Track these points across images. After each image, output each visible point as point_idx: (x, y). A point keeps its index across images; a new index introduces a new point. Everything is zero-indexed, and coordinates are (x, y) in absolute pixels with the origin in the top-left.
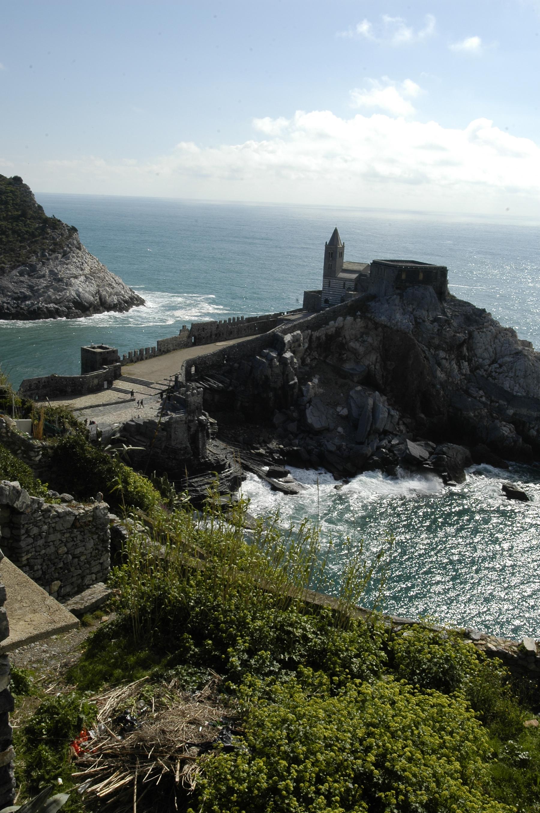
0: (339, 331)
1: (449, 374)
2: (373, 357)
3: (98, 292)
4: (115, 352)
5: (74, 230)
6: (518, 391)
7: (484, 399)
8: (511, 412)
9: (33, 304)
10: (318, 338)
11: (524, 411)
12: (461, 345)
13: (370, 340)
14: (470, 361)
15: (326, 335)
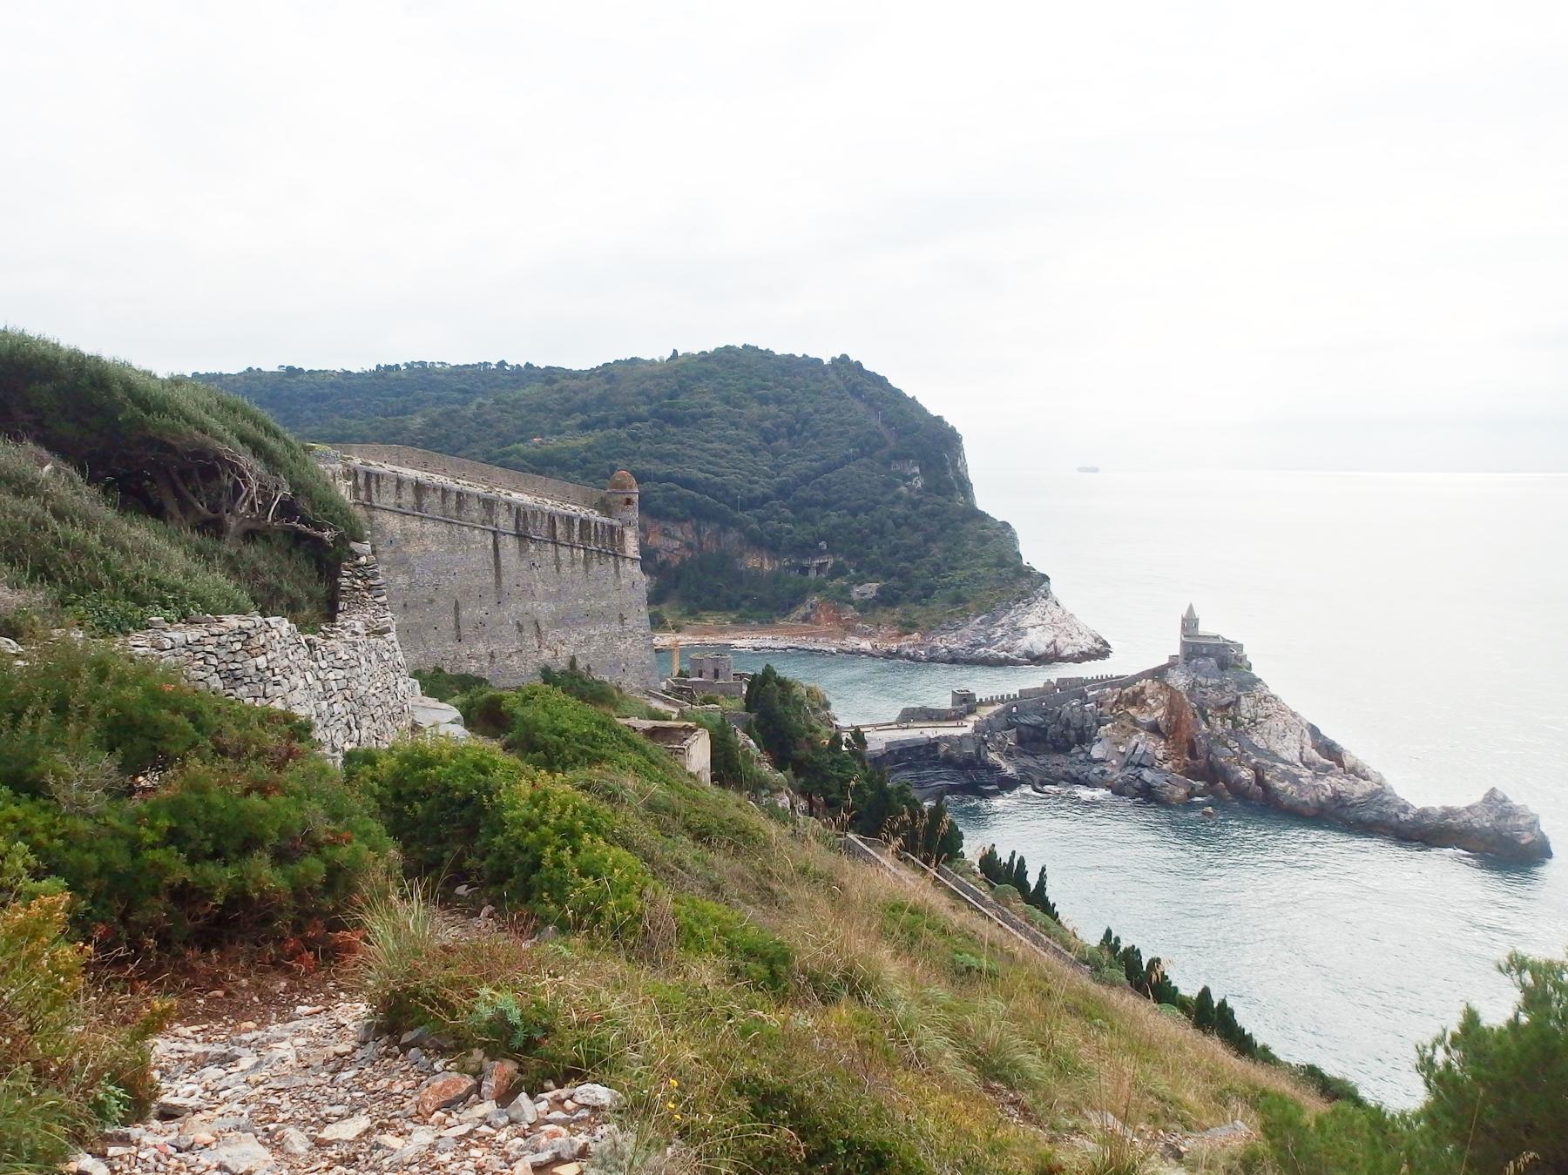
0: (1143, 689)
1: (1213, 729)
2: (1161, 712)
3: (1053, 642)
4: (973, 695)
5: (1045, 578)
6: (1262, 745)
7: (1236, 749)
8: (1253, 761)
9: (986, 652)
10: (1127, 694)
11: (1264, 761)
12: (1229, 705)
13: (1161, 698)
14: (1234, 719)
15: (1134, 692)
